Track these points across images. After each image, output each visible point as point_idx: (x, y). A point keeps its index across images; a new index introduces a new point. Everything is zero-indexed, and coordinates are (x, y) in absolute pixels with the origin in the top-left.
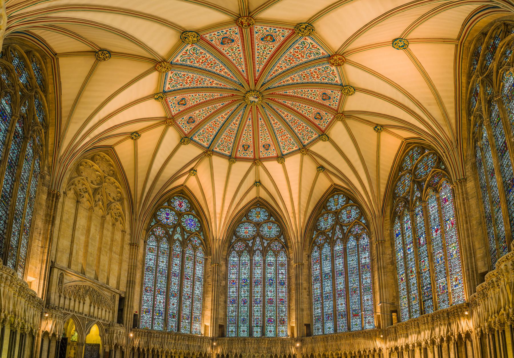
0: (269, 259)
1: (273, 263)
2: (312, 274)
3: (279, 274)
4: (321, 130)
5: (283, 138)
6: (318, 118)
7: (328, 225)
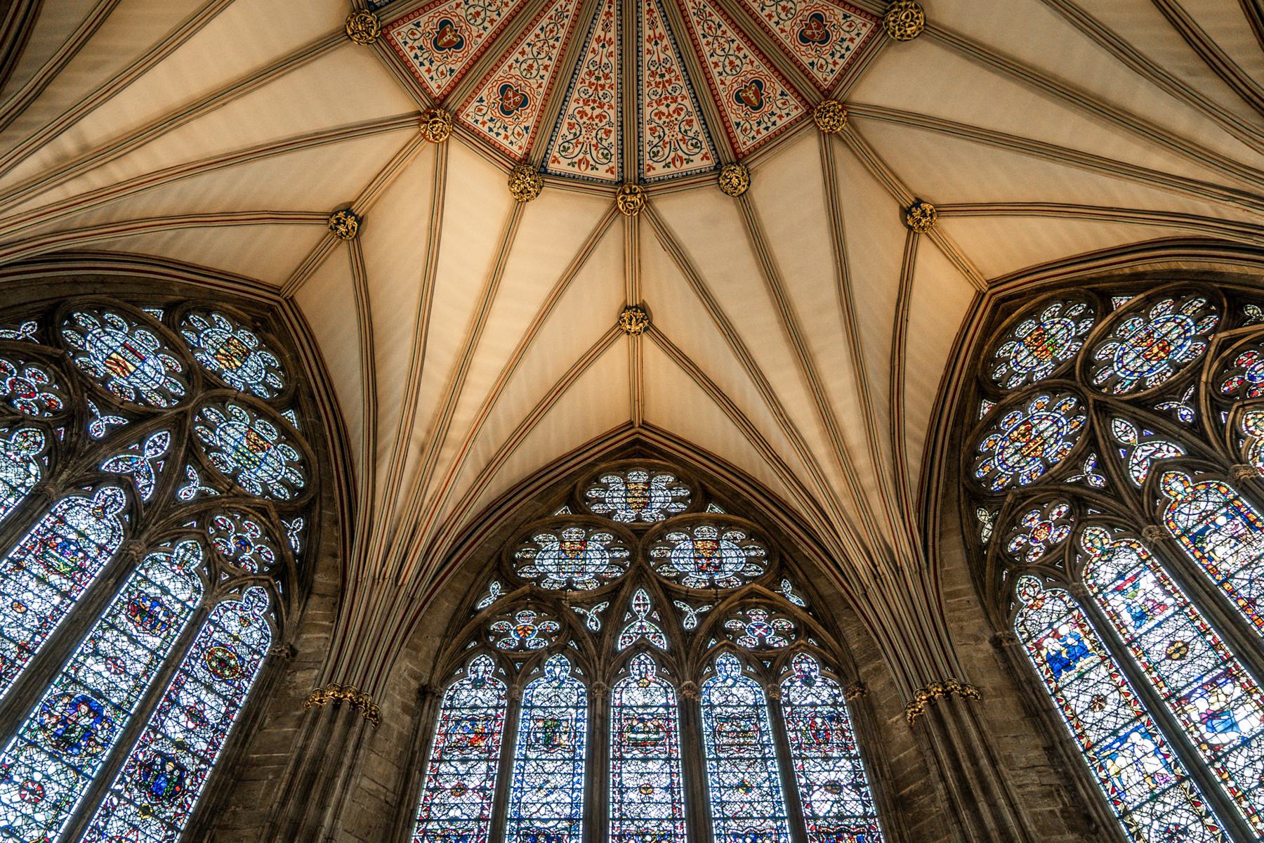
0: (160, 577)
1: (168, 613)
2: (421, 813)
3: (175, 703)
4: (734, 150)
5: (588, 109)
6: (747, 101)
7: (583, 572)
